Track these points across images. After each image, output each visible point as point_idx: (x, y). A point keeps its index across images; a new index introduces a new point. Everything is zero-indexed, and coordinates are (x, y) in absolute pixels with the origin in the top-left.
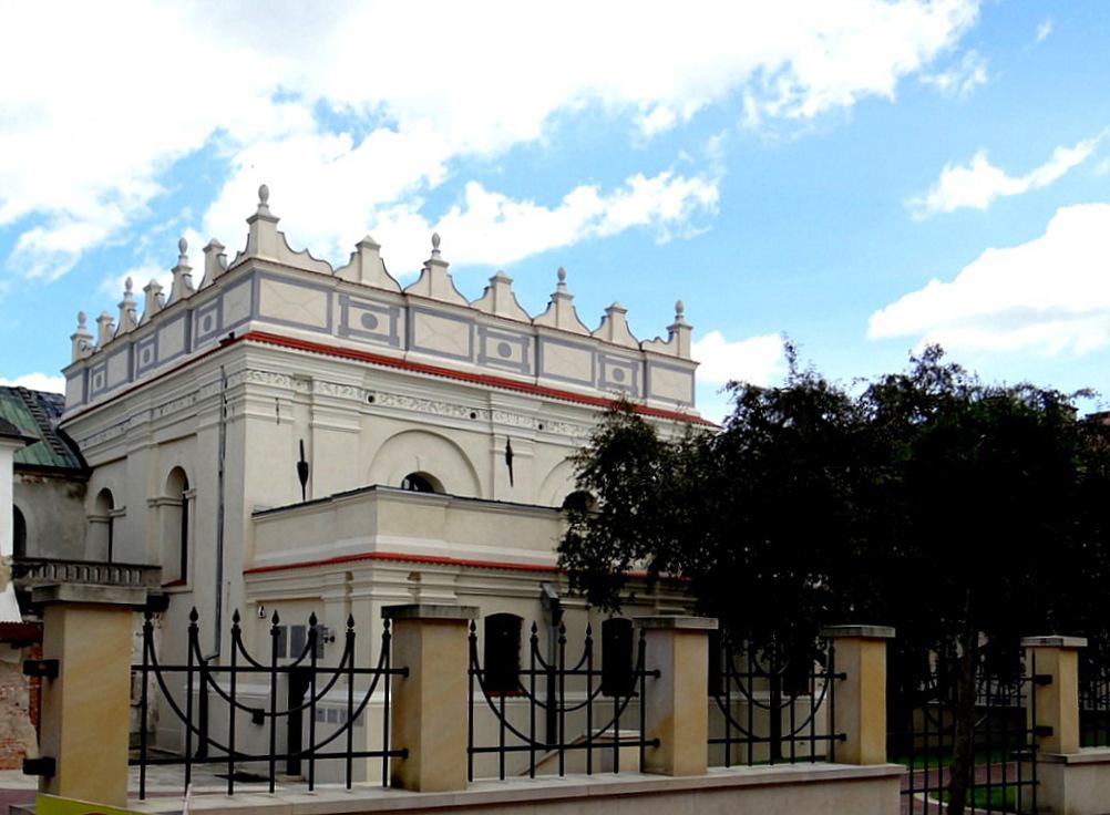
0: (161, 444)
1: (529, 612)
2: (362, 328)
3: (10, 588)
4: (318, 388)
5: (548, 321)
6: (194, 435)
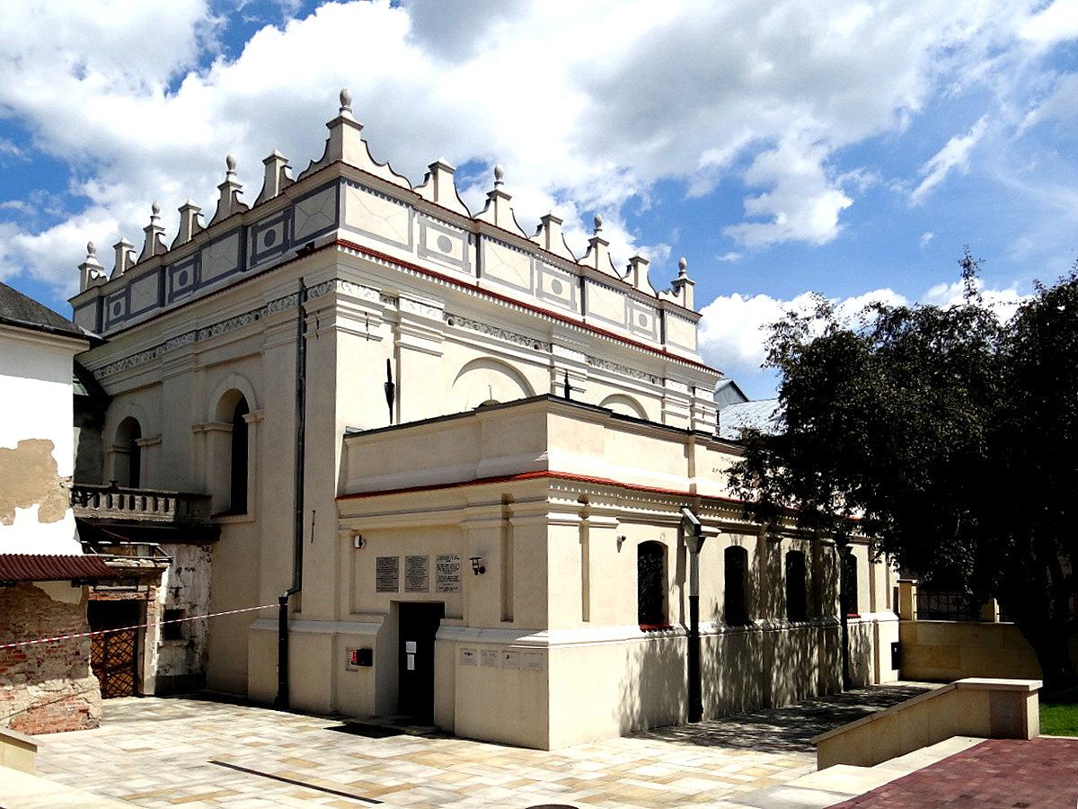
0: (209, 367)
1: (669, 537)
2: (438, 250)
3: (70, 515)
4: (405, 306)
5: (590, 261)
6: (258, 355)
